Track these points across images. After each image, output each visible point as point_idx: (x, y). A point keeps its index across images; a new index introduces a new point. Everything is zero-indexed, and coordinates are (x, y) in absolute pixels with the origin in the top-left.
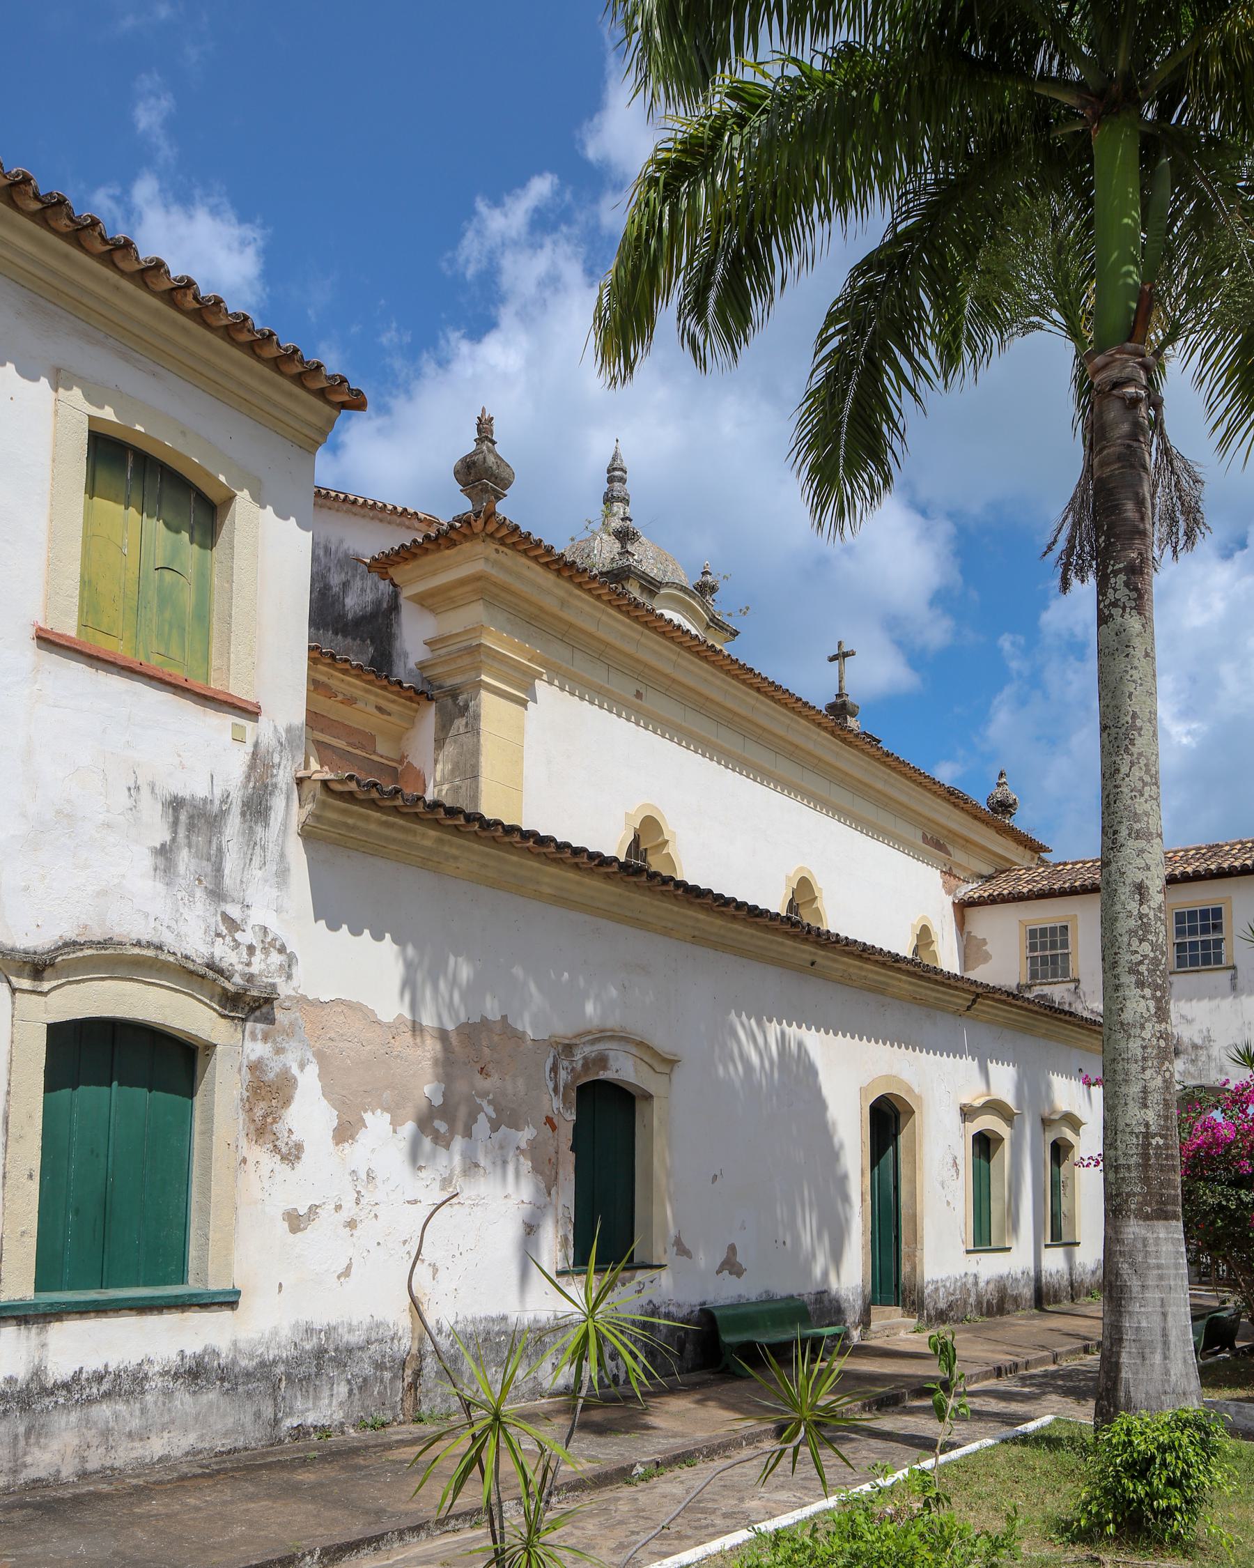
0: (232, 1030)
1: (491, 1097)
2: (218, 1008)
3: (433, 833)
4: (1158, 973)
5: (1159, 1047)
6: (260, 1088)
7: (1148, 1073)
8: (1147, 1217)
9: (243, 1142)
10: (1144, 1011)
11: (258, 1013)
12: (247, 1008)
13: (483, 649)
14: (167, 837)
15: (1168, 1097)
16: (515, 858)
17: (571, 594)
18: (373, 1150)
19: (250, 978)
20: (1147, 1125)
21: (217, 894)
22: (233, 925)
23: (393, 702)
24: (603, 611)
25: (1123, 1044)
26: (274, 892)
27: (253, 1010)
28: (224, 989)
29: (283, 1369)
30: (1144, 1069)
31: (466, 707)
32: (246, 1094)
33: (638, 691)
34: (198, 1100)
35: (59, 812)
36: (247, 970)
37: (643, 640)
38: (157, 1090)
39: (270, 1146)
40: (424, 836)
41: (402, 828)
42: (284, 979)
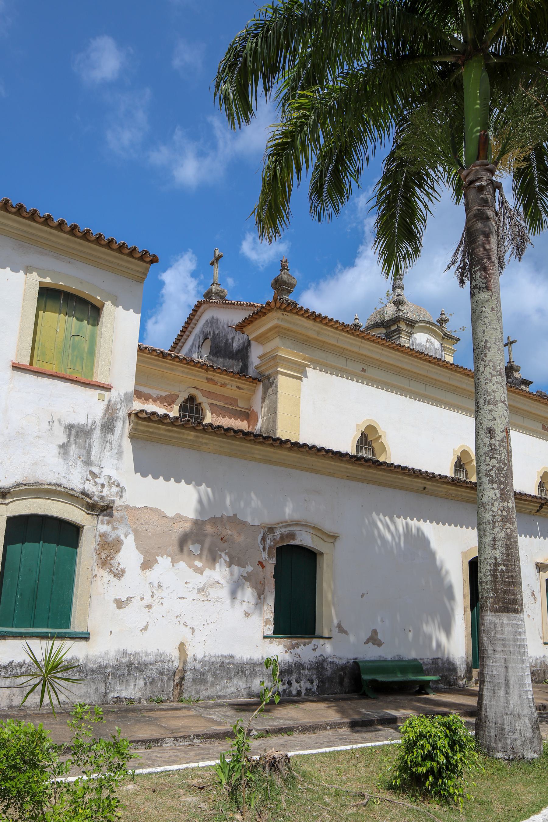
1: (227, 551)
3: (193, 433)
4: (502, 475)
5: (502, 515)
6: (105, 544)
7: (496, 530)
8: (496, 611)
9: (95, 568)
10: (494, 496)
11: (105, 512)
13: (278, 357)
14: (65, 440)
15: (509, 543)
16: (237, 443)
17: (322, 329)
18: (161, 574)
19: (102, 498)
20: (496, 559)
21: (88, 463)
22: (94, 475)
23: (244, 384)
24: (340, 334)
25: (483, 515)
26: (115, 461)
27: (102, 511)
29: (110, 670)
30: (493, 528)
31: (273, 383)
32: (97, 547)
33: (363, 369)
34: (79, 549)
35: (17, 433)
36: (100, 494)
37: (362, 345)
39: (109, 570)
40: (188, 434)
41: (176, 432)
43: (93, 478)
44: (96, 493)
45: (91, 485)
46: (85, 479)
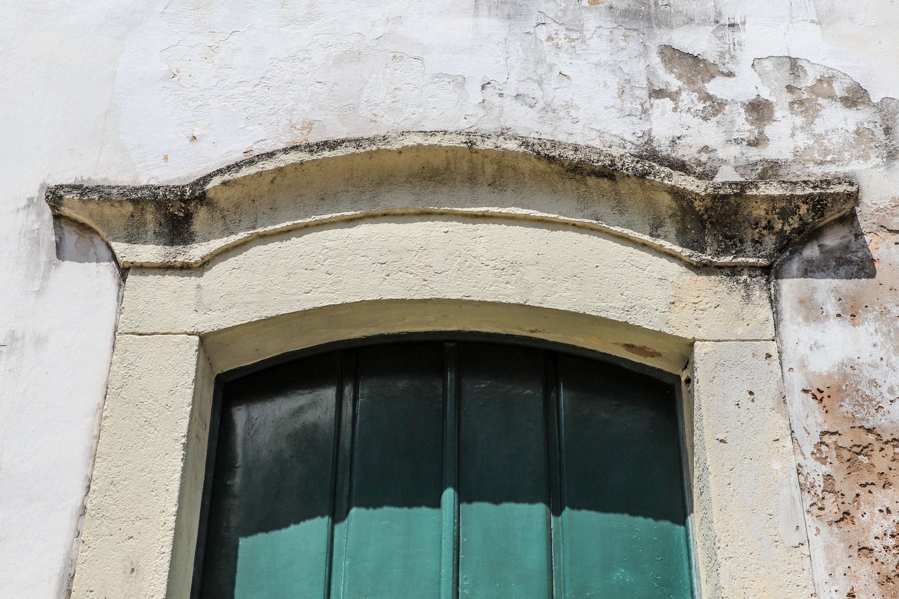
2: (678, 249)
11: (812, 251)
12: (770, 242)
28: (677, 194)
36: (754, 154)
38: (577, 506)
42: (875, 160)
43: (691, 82)
44: (731, 152)
45: (688, 118)
46: (644, 94)
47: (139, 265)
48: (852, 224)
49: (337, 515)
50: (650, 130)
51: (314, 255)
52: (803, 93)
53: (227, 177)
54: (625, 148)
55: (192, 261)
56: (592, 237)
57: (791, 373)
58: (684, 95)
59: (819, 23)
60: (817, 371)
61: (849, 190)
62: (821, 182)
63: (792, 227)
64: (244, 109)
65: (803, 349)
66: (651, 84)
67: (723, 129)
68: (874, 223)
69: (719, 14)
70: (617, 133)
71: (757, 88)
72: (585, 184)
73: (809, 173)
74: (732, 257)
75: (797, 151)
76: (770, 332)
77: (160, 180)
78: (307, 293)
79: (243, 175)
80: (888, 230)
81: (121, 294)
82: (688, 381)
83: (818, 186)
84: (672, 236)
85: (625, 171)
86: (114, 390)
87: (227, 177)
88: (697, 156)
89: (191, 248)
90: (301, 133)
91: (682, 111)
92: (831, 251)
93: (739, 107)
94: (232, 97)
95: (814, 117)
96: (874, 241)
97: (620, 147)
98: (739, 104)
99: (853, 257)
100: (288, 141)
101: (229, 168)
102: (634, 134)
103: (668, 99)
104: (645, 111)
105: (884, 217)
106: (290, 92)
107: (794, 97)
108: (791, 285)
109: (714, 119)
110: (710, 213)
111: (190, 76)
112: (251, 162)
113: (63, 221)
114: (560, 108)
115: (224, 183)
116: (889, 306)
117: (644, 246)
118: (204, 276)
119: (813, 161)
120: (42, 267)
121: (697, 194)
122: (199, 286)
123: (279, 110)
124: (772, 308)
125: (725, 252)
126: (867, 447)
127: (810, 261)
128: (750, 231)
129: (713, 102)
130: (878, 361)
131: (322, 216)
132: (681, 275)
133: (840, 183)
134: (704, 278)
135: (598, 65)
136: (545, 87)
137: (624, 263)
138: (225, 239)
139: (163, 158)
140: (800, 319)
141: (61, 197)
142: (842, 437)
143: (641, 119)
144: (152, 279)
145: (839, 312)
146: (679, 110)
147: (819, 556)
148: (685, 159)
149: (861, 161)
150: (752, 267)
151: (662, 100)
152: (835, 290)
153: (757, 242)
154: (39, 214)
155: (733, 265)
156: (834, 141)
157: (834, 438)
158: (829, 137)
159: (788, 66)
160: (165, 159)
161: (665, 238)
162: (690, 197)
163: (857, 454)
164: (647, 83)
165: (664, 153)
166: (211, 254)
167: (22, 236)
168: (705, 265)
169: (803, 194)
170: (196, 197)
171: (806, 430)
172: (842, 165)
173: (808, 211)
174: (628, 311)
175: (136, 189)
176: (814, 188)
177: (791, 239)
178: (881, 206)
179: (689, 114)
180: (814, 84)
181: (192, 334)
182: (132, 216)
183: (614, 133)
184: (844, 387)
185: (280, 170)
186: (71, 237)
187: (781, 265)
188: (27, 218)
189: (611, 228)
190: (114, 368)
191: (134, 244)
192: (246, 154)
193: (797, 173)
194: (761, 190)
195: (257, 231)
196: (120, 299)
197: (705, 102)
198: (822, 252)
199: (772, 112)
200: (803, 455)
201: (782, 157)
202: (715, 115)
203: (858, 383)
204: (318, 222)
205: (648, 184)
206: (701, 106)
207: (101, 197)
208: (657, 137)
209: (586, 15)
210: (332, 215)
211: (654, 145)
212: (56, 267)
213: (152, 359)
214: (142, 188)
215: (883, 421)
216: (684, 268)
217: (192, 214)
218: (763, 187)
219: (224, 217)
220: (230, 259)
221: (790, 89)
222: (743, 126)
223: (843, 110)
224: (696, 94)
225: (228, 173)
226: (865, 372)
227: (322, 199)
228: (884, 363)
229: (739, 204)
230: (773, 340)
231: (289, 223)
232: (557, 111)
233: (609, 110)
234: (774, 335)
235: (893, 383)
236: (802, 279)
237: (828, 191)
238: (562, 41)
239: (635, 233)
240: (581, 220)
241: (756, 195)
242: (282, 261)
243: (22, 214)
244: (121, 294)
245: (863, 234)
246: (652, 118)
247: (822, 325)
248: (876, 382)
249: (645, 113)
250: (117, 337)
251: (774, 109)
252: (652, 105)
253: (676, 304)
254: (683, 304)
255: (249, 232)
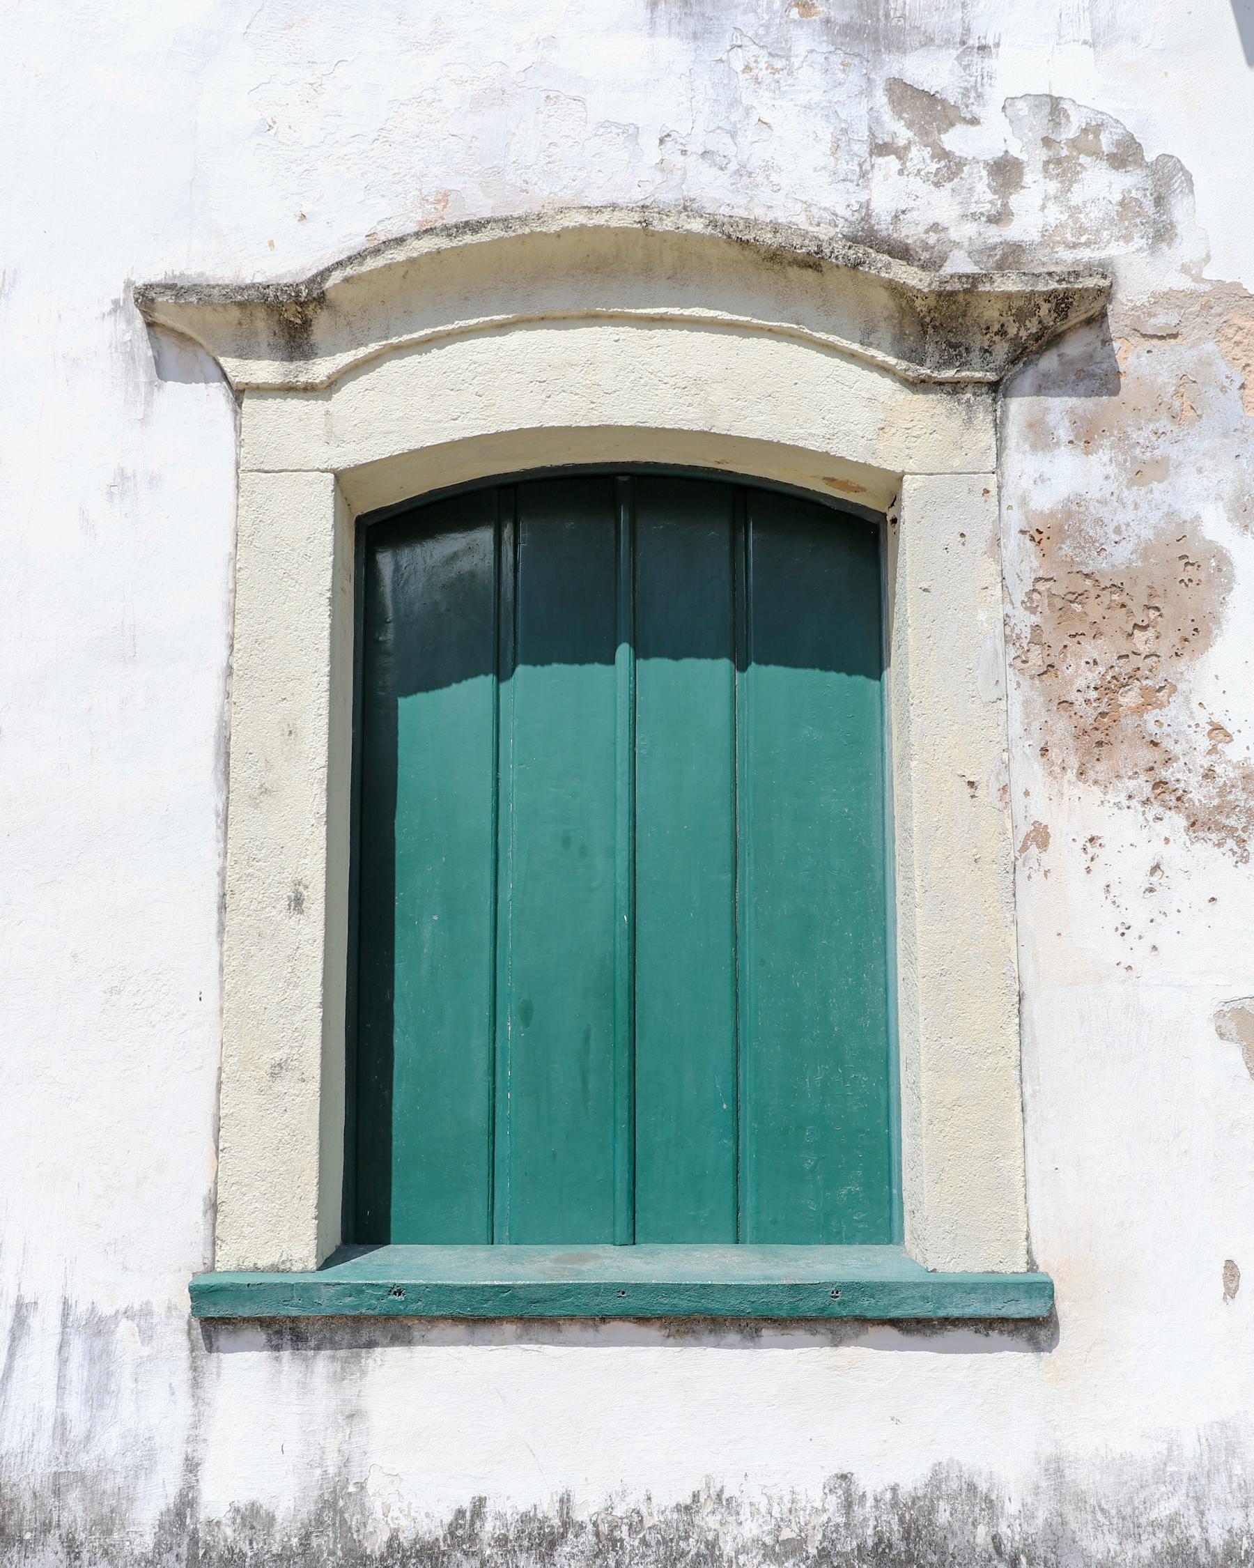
0: (956, 423)
2: (892, 360)
11: (1049, 362)
12: (1002, 350)
19: (1012, 255)
28: (896, 290)
36: (995, 234)
42: (1139, 242)
43: (923, 132)
44: (964, 232)
45: (916, 184)
46: (862, 149)
47: (254, 386)
48: (1101, 327)
49: (502, 673)
50: (868, 202)
51: (460, 371)
52: (1062, 148)
53: (349, 271)
54: (836, 226)
55: (317, 381)
56: (791, 345)
57: (1010, 511)
58: (914, 152)
59: (1093, 45)
60: (1039, 509)
61: (1101, 284)
62: (1069, 273)
63: (1029, 332)
64: (362, 174)
65: (1026, 483)
66: (873, 135)
67: (959, 199)
68: (1126, 326)
69: (967, 31)
70: (827, 205)
71: (1005, 141)
72: (785, 277)
73: (1057, 259)
74: (955, 371)
75: (1046, 230)
76: (991, 463)
77: (267, 274)
78: (454, 420)
79: (368, 269)
80: (1141, 334)
81: (238, 422)
82: (894, 521)
83: (1064, 280)
84: (887, 344)
85: (834, 260)
86: (245, 538)
87: (349, 271)
88: (924, 236)
89: (313, 363)
90: (435, 209)
91: (910, 173)
92: (1072, 362)
93: (981, 168)
94: (346, 158)
95: (1072, 182)
96: (1124, 348)
97: (830, 224)
98: (982, 164)
99: (1097, 370)
100: (420, 219)
101: (350, 260)
102: (849, 206)
103: (893, 157)
104: (863, 175)
105: (1139, 317)
106: (418, 150)
107: (1051, 153)
108: (1021, 405)
109: (949, 185)
110: (932, 314)
111: (290, 127)
112: (376, 251)
113: (158, 329)
114: (758, 170)
115: (347, 280)
116: (1129, 429)
117: (851, 357)
118: (333, 399)
119: (1064, 243)
120: (143, 389)
121: (919, 290)
122: (327, 413)
123: (405, 175)
124: (996, 434)
125: (947, 364)
126: (1082, 594)
127: (1045, 375)
128: (979, 336)
129: (950, 162)
130: (1108, 496)
131: (467, 322)
132: (894, 394)
133: (1091, 276)
134: (920, 397)
135: (807, 107)
136: (740, 140)
137: (828, 379)
138: (353, 352)
139: (267, 244)
140: (1027, 447)
141: (153, 300)
142: (1057, 583)
143: (858, 185)
144: (273, 405)
145: (1071, 438)
146: (906, 173)
147: (1016, 710)
148: (909, 241)
149: (1121, 243)
150: (978, 383)
151: (886, 158)
152: (1072, 411)
153: (986, 351)
154: (129, 322)
155: (956, 380)
156: (1092, 216)
157: (1048, 584)
158: (1087, 210)
159: (1048, 109)
160: (270, 245)
161: (878, 347)
162: (911, 294)
163: (1071, 602)
164: (868, 134)
165: (884, 233)
166: (338, 371)
167: (113, 350)
168: (923, 381)
169: (1046, 289)
170: (314, 299)
171: (1019, 577)
172: (1098, 249)
173: (1050, 311)
174: (829, 439)
175: (242, 289)
176: (1059, 281)
177: (1027, 347)
178: (1138, 304)
179: (918, 178)
180: (1077, 134)
181: (326, 471)
182: (240, 324)
183: (823, 205)
184: (1066, 527)
185: (412, 261)
186: (171, 351)
187: (1012, 380)
188: (115, 327)
189: (815, 334)
190: (242, 512)
191: (246, 359)
192: (370, 238)
193: (1043, 259)
194: (996, 284)
195: (390, 342)
196: (238, 429)
197: (939, 161)
198: (1062, 364)
199: (1021, 174)
200: (1012, 604)
201: (1032, 235)
202: (950, 180)
203: (1081, 522)
204: (462, 330)
205: (861, 277)
206: (933, 167)
207: (200, 299)
208: (876, 211)
209: (795, 32)
210: (478, 320)
211: (873, 222)
212: (158, 389)
213: (283, 502)
214: (248, 287)
215: (1103, 565)
216: (898, 384)
217: (311, 321)
218: (999, 280)
219: (349, 324)
220: (361, 378)
221: (1047, 142)
222: (983, 195)
223: (1108, 172)
224: (929, 149)
225: (350, 266)
226: (1092, 509)
227: (466, 298)
228: (1114, 498)
229: (969, 303)
230: (993, 473)
231: (428, 331)
232: (753, 175)
233: (819, 173)
234: (995, 466)
235: (1121, 522)
236: (1035, 398)
237: (1076, 286)
238: (764, 74)
239: (842, 340)
240: (779, 324)
241: (989, 291)
242: (422, 379)
243: (110, 320)
244: (238, 422)
245: (1112, 340)
246: (872, 185)
247: (1051, 454)
248: (1102, 521)
249: (863, 177)
250: (241, 475)
251: (1025, 170)
252: (873, 166)
253: (886, 430)
254: (894, 430)
255: (380, 343)
